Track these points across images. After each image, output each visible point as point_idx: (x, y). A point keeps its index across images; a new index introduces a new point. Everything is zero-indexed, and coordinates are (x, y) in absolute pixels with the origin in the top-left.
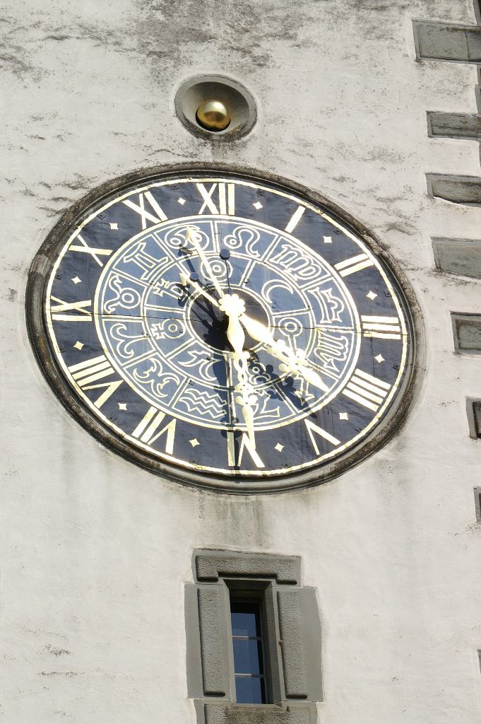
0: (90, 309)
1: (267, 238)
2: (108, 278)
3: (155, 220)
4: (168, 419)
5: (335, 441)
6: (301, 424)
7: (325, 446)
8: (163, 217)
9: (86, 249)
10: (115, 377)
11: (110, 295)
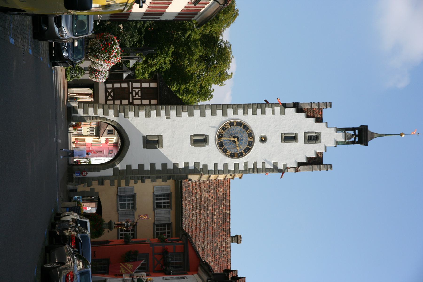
0: (235, 125)
2: (239, 127)
3: (247, 132)
4: (223, 133)
5: (222, 150)
6: (223, 146)
7: (221, 149)
8: (248, 133)
9: (243, 125)
10: (228, 128)
11: (237, 127)
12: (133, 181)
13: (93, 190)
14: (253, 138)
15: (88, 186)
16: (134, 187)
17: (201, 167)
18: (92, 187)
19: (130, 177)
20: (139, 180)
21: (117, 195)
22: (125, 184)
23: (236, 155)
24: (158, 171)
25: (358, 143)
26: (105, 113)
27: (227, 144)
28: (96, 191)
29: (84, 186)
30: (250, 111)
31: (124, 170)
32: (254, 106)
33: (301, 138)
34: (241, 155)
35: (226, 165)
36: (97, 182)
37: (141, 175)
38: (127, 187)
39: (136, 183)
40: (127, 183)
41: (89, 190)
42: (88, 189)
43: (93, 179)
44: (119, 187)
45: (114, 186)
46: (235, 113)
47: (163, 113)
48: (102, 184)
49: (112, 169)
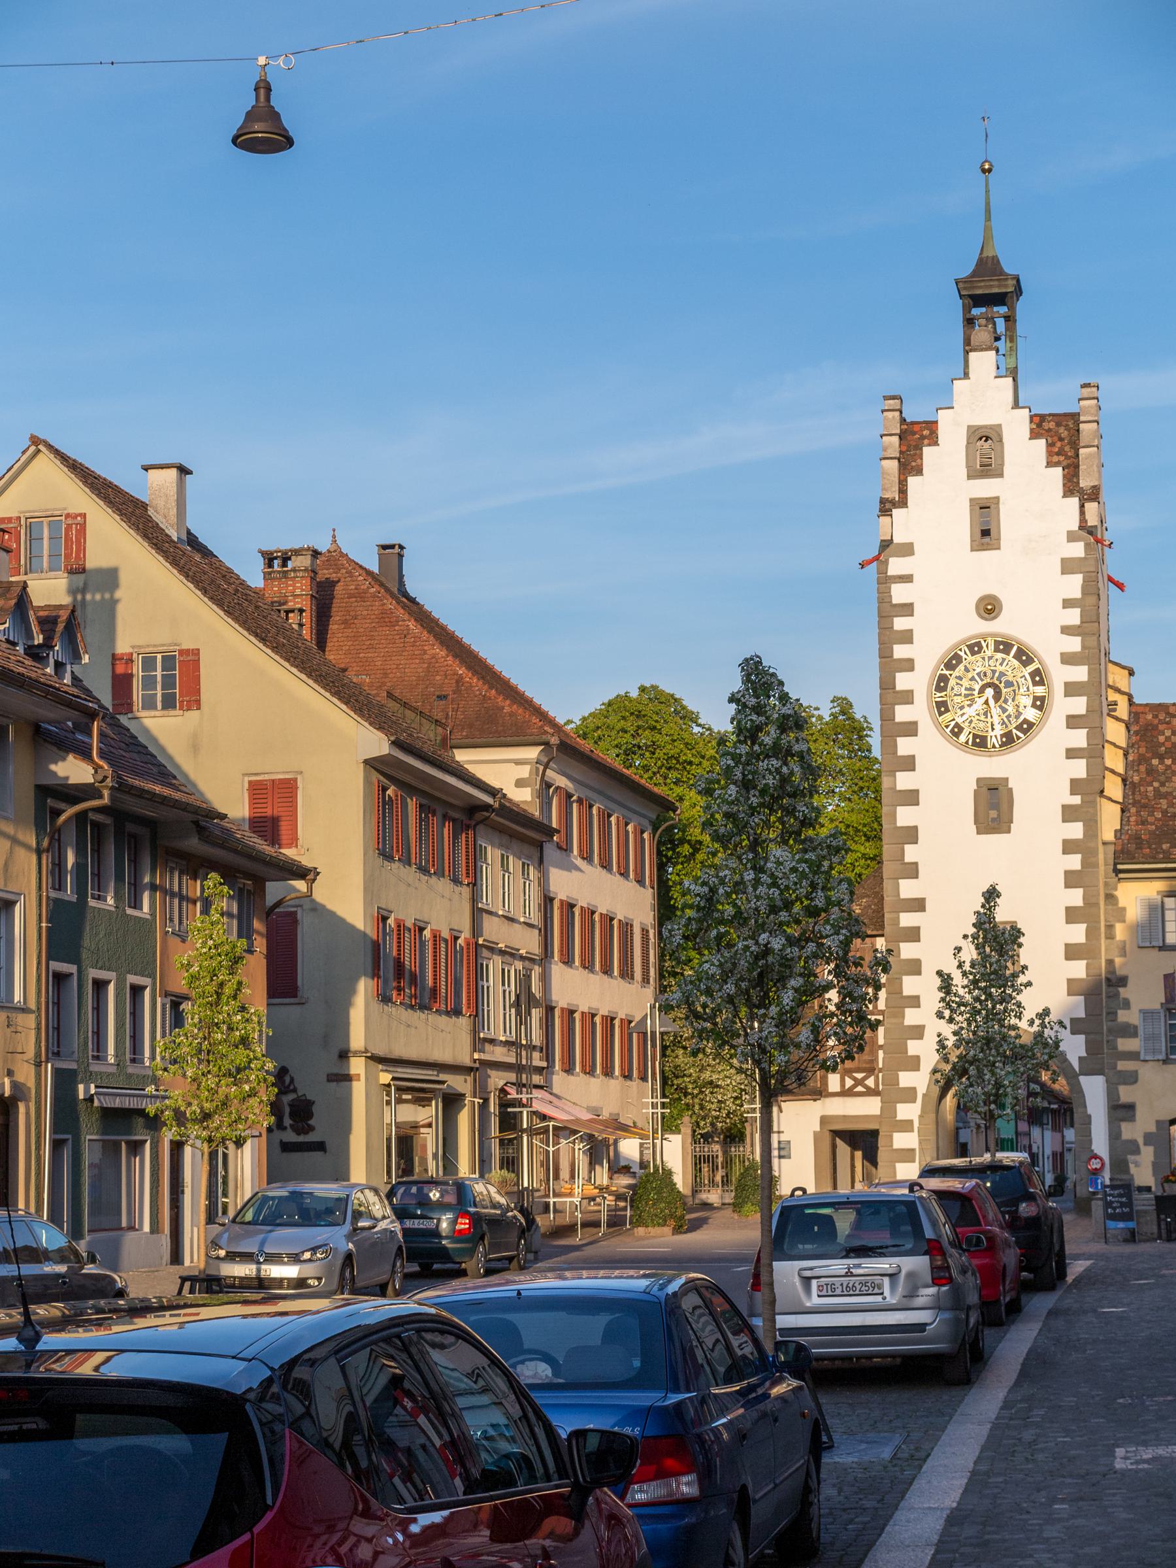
1: (1004, 660)
7: (1019, 738)
11: (953, 689)
12: (1120, 1012)
13: (1149, 1139)
14: (984, 637)
15: (1137, 1151)
16: (1140, 1011)
17: (1077, 800)
18: (1141, 1141)
19: (1110, 1023)
20: (1117, 994)
21: (1166, 1061)
22: (1130, 1036)
23: (1040, 691)
24: (1091, 933)
25: (1012, 308)
26: (909, 1095)
27: (1006, 720)
28: (1153, 1128)
29: (1137, 1164)
30: (900, 651)
31: (1087, 1042)
32: (888, 638)
33: (985, 488)
34: (1039, 677)
35: (1073, 722)
36: (1124, 1126)
37: (1104, 987)
38: (1141, 1032)
39: (1127, 1005)
40: (1129, 1031)
41: (1151, 1149)
42: (1147, 1154)
43: (1114, 1136)
44: (1142, 1058)
45: (1136, 1072)
46: (907, 697)
47: (907, 920)
48: (1131, 1107)
49: (1082, 1079)
